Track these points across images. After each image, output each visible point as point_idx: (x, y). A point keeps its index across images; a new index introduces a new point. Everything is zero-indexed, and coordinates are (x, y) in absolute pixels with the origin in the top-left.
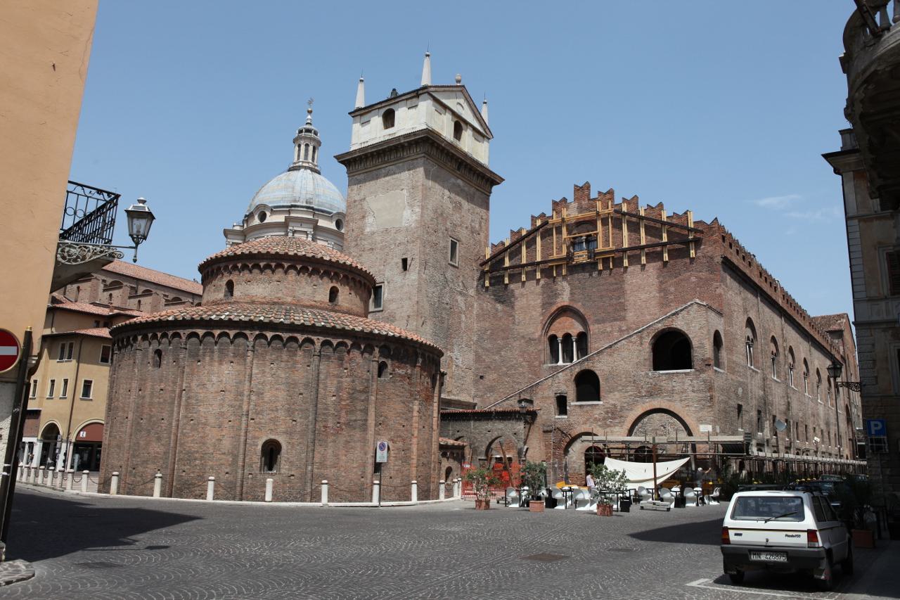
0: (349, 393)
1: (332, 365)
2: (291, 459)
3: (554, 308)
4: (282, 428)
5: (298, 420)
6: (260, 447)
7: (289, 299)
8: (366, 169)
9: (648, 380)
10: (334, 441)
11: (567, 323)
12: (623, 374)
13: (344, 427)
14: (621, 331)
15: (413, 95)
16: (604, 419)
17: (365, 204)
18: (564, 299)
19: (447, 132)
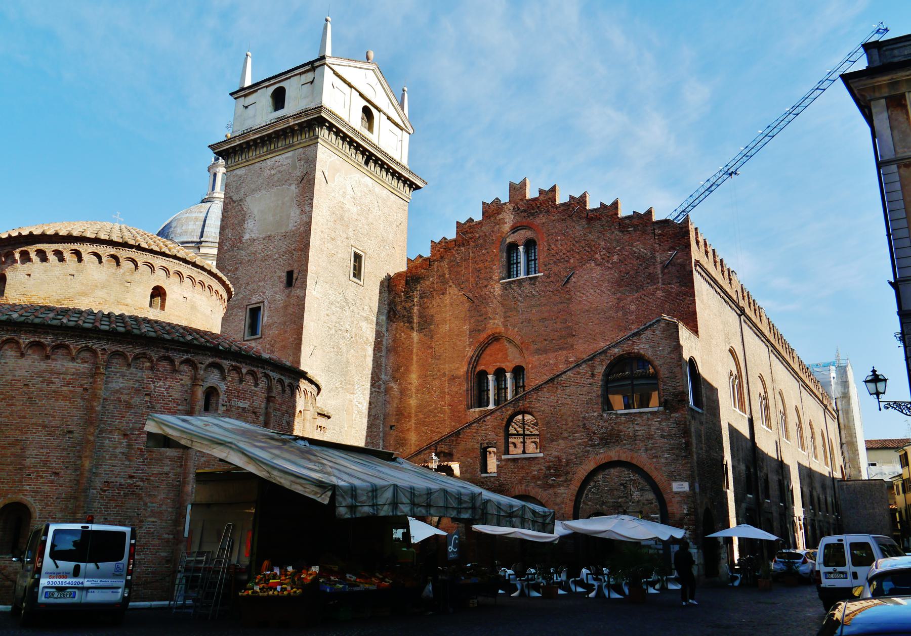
3: (483, 336)
8: (247, 161)
9: (602, 423)
11: (500, 356)
12: (570, 416)
15: (307, 68)
16: (546, 477)
17: (245, 206)
19: (356, 120)
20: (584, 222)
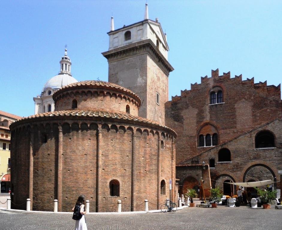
0: (149, 156)
1: (142, 142)
2: (125, 190)
3: (202, 124)
4: (119, 174)
5: (127, 170)
6: (108, 184)
7: (108, 110)
10: (144, 180)
13: (148, 173)
14: (234, 132)
18: (207, 119)
20: (241, 85)
